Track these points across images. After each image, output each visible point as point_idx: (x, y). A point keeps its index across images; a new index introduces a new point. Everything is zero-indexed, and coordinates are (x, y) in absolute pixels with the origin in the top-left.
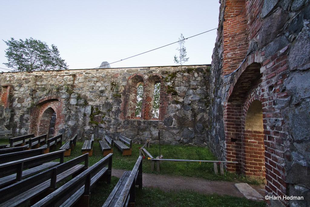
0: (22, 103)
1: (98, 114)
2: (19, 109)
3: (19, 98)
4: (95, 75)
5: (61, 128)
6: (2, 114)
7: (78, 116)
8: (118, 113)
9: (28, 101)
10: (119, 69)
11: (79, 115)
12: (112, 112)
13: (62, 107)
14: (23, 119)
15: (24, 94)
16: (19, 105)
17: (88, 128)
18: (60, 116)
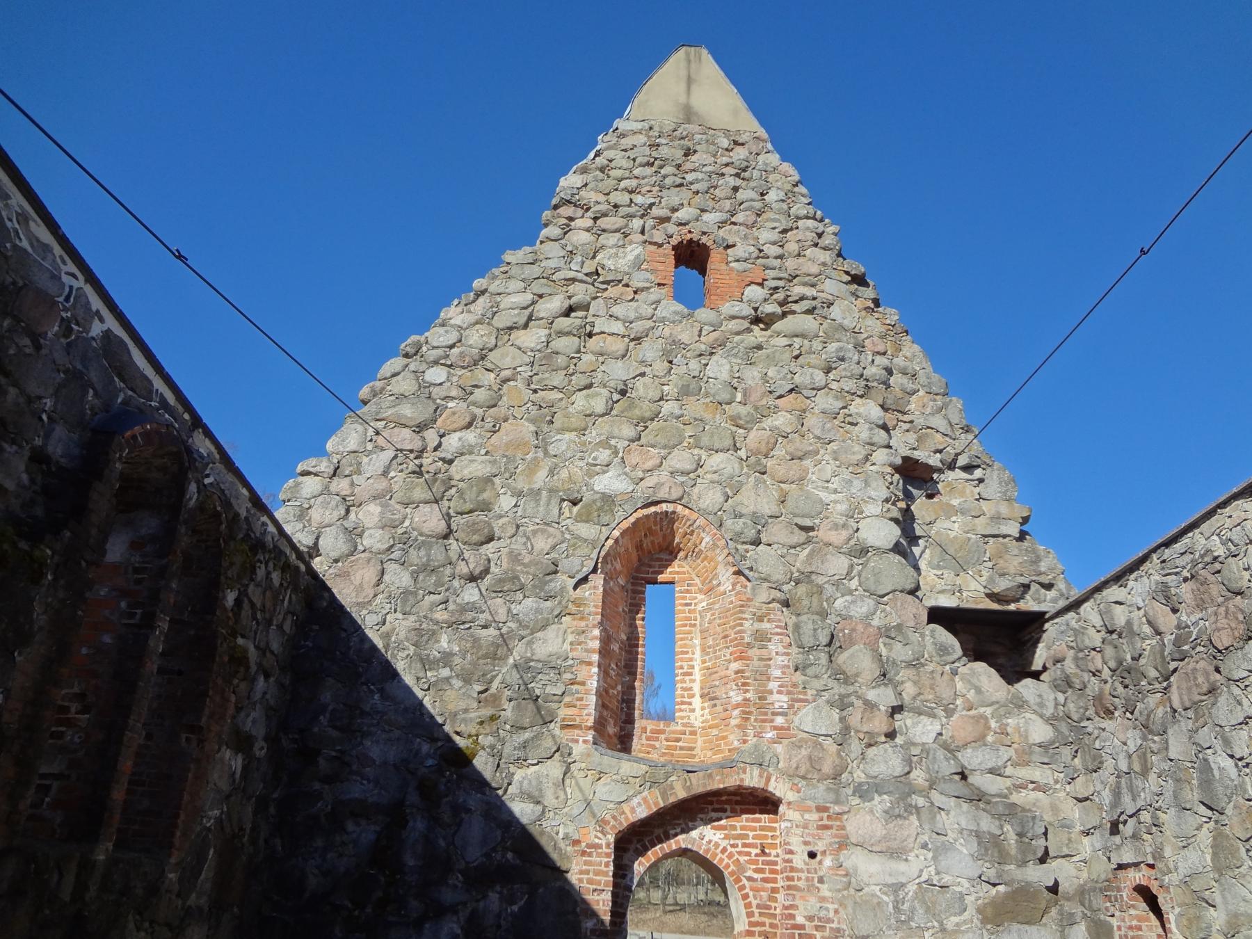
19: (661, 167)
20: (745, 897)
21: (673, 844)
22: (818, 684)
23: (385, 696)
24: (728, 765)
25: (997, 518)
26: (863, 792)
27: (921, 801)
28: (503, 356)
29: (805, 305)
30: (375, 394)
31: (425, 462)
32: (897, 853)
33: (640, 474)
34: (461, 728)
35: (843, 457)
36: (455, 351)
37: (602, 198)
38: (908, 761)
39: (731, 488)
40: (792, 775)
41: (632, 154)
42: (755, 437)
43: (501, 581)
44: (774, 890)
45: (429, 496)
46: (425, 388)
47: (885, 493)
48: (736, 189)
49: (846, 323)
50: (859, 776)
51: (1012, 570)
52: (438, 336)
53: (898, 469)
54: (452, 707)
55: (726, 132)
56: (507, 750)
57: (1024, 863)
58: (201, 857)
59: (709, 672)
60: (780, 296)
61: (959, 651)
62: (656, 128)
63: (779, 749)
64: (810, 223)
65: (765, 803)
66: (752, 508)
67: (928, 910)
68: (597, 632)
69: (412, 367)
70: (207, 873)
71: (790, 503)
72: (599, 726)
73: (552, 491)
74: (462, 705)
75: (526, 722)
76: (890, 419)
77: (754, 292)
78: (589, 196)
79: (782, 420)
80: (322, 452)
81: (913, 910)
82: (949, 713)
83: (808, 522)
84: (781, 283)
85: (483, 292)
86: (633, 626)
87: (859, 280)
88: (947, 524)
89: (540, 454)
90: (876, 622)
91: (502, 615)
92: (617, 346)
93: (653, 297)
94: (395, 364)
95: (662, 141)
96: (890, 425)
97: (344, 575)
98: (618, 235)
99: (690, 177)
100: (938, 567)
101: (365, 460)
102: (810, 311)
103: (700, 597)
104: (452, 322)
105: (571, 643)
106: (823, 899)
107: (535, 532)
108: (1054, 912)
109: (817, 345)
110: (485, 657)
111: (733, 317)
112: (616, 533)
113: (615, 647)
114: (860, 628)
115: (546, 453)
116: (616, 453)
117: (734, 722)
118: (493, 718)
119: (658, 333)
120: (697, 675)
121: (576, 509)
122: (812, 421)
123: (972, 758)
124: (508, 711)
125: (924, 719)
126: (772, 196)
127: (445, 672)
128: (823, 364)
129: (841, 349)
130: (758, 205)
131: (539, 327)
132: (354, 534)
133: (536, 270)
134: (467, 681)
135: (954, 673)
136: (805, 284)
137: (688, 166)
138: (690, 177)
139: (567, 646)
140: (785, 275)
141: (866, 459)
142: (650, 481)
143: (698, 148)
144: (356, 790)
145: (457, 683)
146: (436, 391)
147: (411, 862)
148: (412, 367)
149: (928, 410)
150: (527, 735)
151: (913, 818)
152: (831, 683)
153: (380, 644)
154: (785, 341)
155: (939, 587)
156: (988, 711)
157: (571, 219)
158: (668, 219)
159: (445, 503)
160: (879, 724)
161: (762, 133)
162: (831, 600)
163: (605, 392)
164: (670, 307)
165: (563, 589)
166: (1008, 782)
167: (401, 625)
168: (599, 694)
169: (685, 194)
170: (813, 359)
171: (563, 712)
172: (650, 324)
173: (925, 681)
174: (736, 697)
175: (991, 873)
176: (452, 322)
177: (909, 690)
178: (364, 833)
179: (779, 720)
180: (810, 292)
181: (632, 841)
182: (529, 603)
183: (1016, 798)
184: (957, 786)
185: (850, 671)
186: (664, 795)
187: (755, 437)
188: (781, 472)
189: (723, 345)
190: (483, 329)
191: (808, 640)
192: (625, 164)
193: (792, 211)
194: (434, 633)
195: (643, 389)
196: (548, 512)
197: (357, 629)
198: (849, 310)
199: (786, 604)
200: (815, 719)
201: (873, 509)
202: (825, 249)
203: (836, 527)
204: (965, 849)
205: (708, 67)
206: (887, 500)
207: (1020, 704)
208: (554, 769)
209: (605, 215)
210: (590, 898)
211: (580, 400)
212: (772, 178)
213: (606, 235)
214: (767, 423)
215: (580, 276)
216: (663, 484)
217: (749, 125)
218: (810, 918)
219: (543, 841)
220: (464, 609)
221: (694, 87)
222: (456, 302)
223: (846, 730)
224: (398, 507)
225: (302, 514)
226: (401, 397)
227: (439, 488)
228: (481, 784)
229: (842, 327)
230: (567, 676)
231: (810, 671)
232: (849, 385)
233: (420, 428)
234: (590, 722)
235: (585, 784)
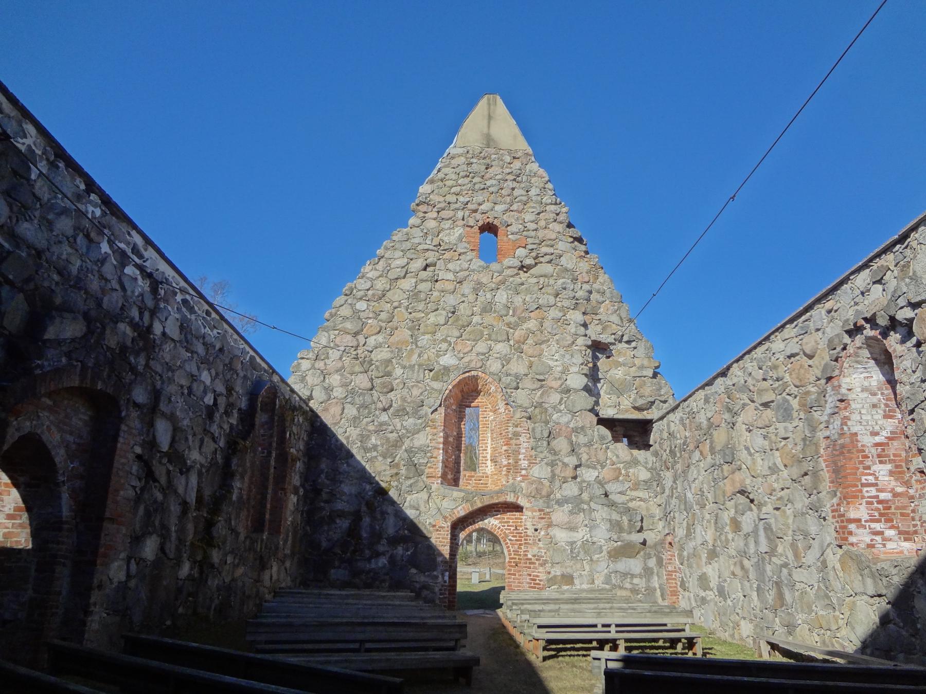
10: (242, 342)
11: (172, 508)
19: (473, 178)
20: (508, 547)
21: (477, 526)
22: (542, 456)
23: (348, 465)
24: (500, 492)
25: (642, 367)
26: (560, 503)
27: (586, 507)
28: (394, 294)
29: (548, 258)
30: (332, 315)
31: (360, 352)
32: (573, 529)
33: (462, 355)
34: (383, 478)
35: (561, 343)
36: (370, 292)
37: (442, 199)
38: (581, 489)
39: (505, 360)
40: (528, 496)
41: (457, 170)
42: (518, 334)
43: (398, 411)
44: (521, 545)
45: (362, 369)
46: (356, 312)
47: (581, 361)
48: (513, 189)
49: (568, 266)
50: (558, 496)
51: (647, 394)
52: (362, 284)
53: (589, 347)
54: (379, 469)
55: (510, 152)
56: (403, 488)
57: (630, 533)
58: (288, 536)
59: (494, 449)
60: (534, 254)
61: (610, 438)
62: (471, 152)
63: (523, 484)
64: (553, 207)
65: (518, 508)
66: (515, 371)
67: (585, 552)
68: (442, 434)
69: (349, 301)
70: (289, 542)
71: (533, 368)
72: (444, 476)
73: (420, 365)
74: (383, 468)
75: (411, 475)
76: (587, 318)
77: (521, 252)
78: (435, 198)
79: (532, 324)
80: (309, 348)
81: (579, 552)
82: (603, 467)
83: (542, 377)
84: (534, 246)
85: (382, 257)
86: (460, 428)
87: (579, 240)
88: (616, 372)
89: (414, 347)
90: (572, 425)
91: (399, 427)
92: (450, 286)
93: (469, 258)
94: (340, 300)
95: (474, 160)
96: (588, 322)
97: (326, 410)
98: (450, 222)
99: (488, 183)
100: (610, 394)
101: (331, 352)
102: (550, 262)
103: (491, 414)
104: (368, 275)
105: (430, 440)
106: (540, 548)
107: (412, 387)
108: (642, 553)
109: (552, 282)
110: (392, 446)
111: (510, 267)
112: (450, 387)
113: (451, 439)
114: (564, 428)
115: (417, 346)
116: (450, 345)
117: (504, 473)
118: (397, 474)
119: (471, 278)
120: (489, 451)
121: (432, 374)
122: (547, 324)
123: (610, 487)
124: (403, 471)
125: (590, 470)
126: (533, 192)
127: (375, 454)
128: (553, 292)
129: (564, 283)
130: (525, 198)
131: (411, 277)
132: (328, 390)
133: (408, 245)
134: (385, 458)
135: (608, 448)
136: (547, 246)
137: (488, 176)
138: (488, 183)
139: (428, 441)
140: (537, 241)
141: (573, 343)
142: (466, 359)
143: (493, 163)
144: (340, 506)
145: (380, 459)
146: (362, 315)
147: (365, 535)
148: (349, 301)
149: (610, 312)
150: (412, 481)
151: (582, 514)
152: (548, 455)
153: (345, 442)
154: (535, 280)
155: (609, 404)
156: (622, 465)
157: (425, 213)
158: (475, 211)
159: (370, 373)
160: (569, 473)
161: (530, 151)
162: (551, 416)
163: (444, 313)
164: (478, 263)
165: (426, 414)
166: (628, 498)
167: (354, 433)
168: (443, 462)
169: (486, 194)
170: (549, 290)
171: (427, 471)
172: (467, 273)
173: (593, 452)
174: (505, 462)
175: (615, 537)
176: (368, 275)
177: (585, 457)
178: (344, 524)
179: (524, 472)
180: (550, 250)
181: (459, 525)
182: (411, 420)
183: (631, 505)
184: (604, 500)
185: (557, 449)
186: (472, 505)
187: (518, 334)
188: (530, 352)
189: (504, 283)
190: (383, 280)
191: (538, 435)
192: (454, 177)
193: (544, 201)
194: (369, 436)
195: (463, 310)
196: (418, 375)
197: (334, 435)
198: (571, 258)
199: (530, 418)
200: (540, 471)
201: (575, 369)
202: (561, 223)
203: (556, 379)
204: (604, 527)
205: (501, 108)
206: (582, 364)
207: (635, 462)
208: (424, 495)
209: (443, 209)
210: (440, 548)
211: (432, 318)
212: (533, 180)
213: (444, 222)
214: (525, 326)
215: (431, 247)
216: (472, 359)
217: (522, 145)
218: (534, 556)
219: (420, 526)
220: (381, 424)
221: (492, 122)
222: (368, 262)
223: (554, 475)
224: (349, 375)
225: (303, 379)
226: (345, 319)
227: (366, 364)
228: (393, 503)
229: (566, 270)
230: (429, 455)
231: (538, 450)
232: (566, 303)
233: (356, 334)
234: (440, 475)
235: (438, 501)
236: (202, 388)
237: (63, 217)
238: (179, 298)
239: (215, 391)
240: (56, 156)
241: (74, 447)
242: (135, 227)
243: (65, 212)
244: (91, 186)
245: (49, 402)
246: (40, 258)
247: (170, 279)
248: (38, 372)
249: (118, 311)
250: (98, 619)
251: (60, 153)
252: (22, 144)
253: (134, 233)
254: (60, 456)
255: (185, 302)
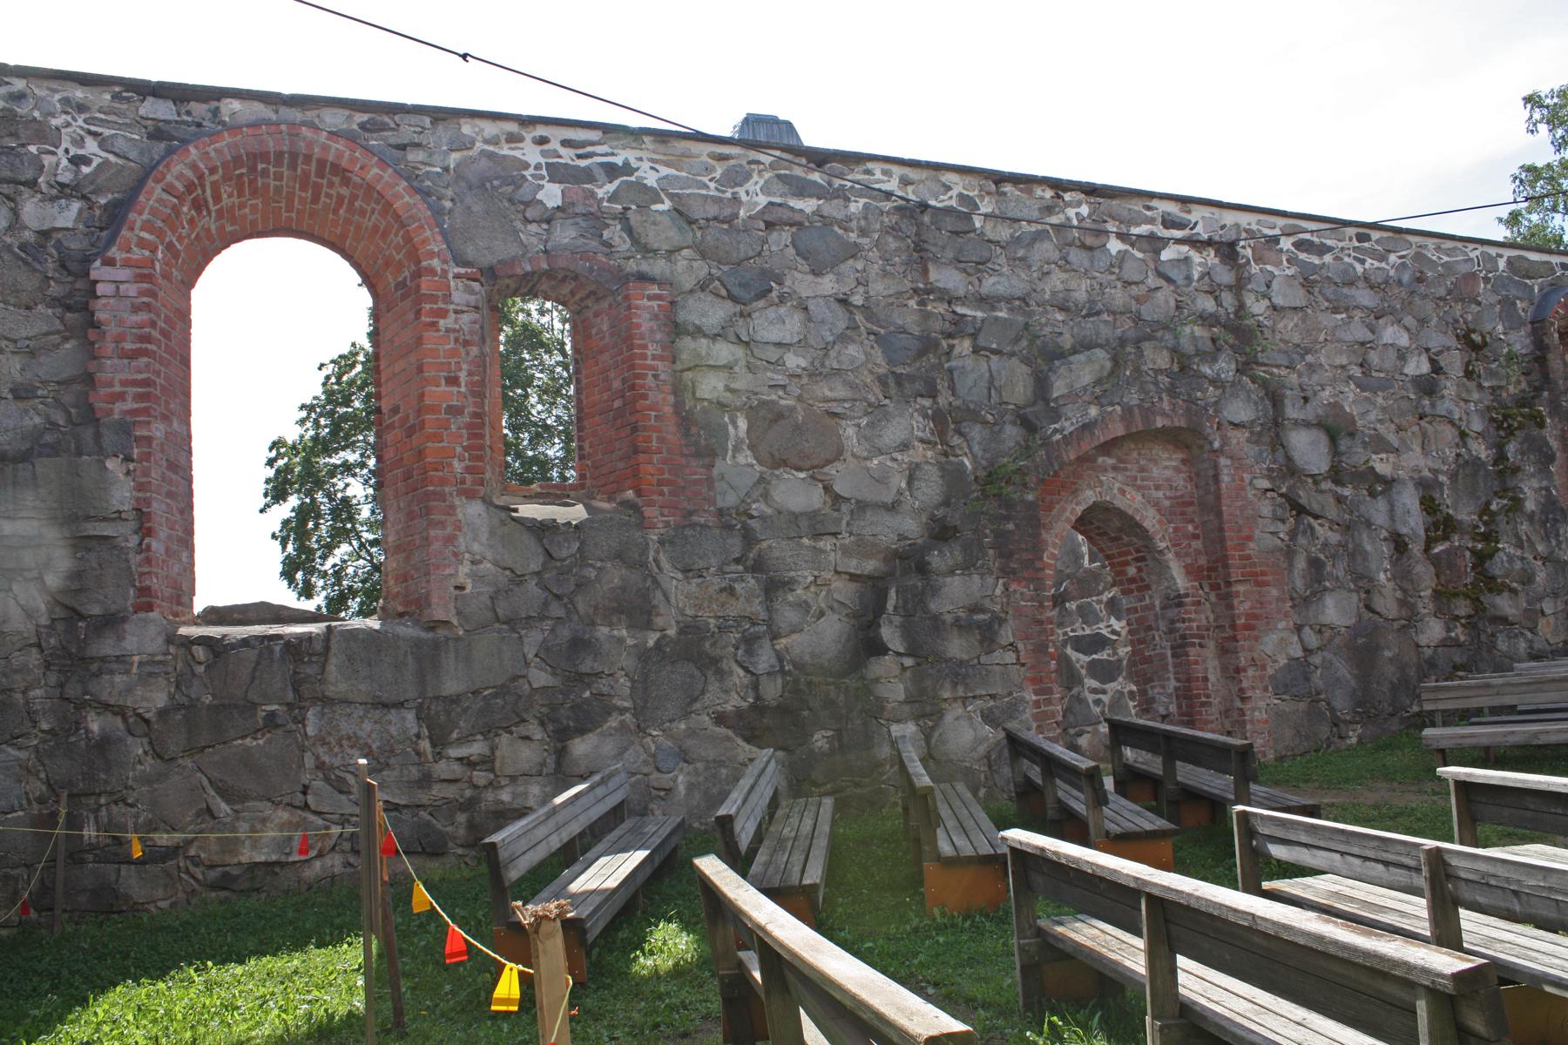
0: (830, 470)
1: (1446, 538)
2: (816, 525)
3: (766, 416)
4: (1359, 268)
5: (1283, 661)
6: (645, 595)
7: (1365, 555)
8: (1556, 521)
9: (904, 447)
11: (1369, 548)
12: (1531, 517)
13: (1250, 493)
14: (936, 618)
15: (814, 374)
16: (796, 493)
17: (1433, 631)
18: (1254, 564)
236: (1392, 354)
237: (1037, 245)
238: (1286, 244)
239: (1427, 350)
240: (997, 183)
241: (1167, 503)
242: (1152, 195)
243: (1040, 236)
244: (1059, 186)
245: (1110, 461)
246: (1027, 305)
247: (1254, 227)
248: (1058, 436)
249: (1172, 312)
250: (1261, 705)
251: (999, 178)
252: (948, 200)
253: (1154, 203)
254: (1150, 520)
255: (1299, 245)
